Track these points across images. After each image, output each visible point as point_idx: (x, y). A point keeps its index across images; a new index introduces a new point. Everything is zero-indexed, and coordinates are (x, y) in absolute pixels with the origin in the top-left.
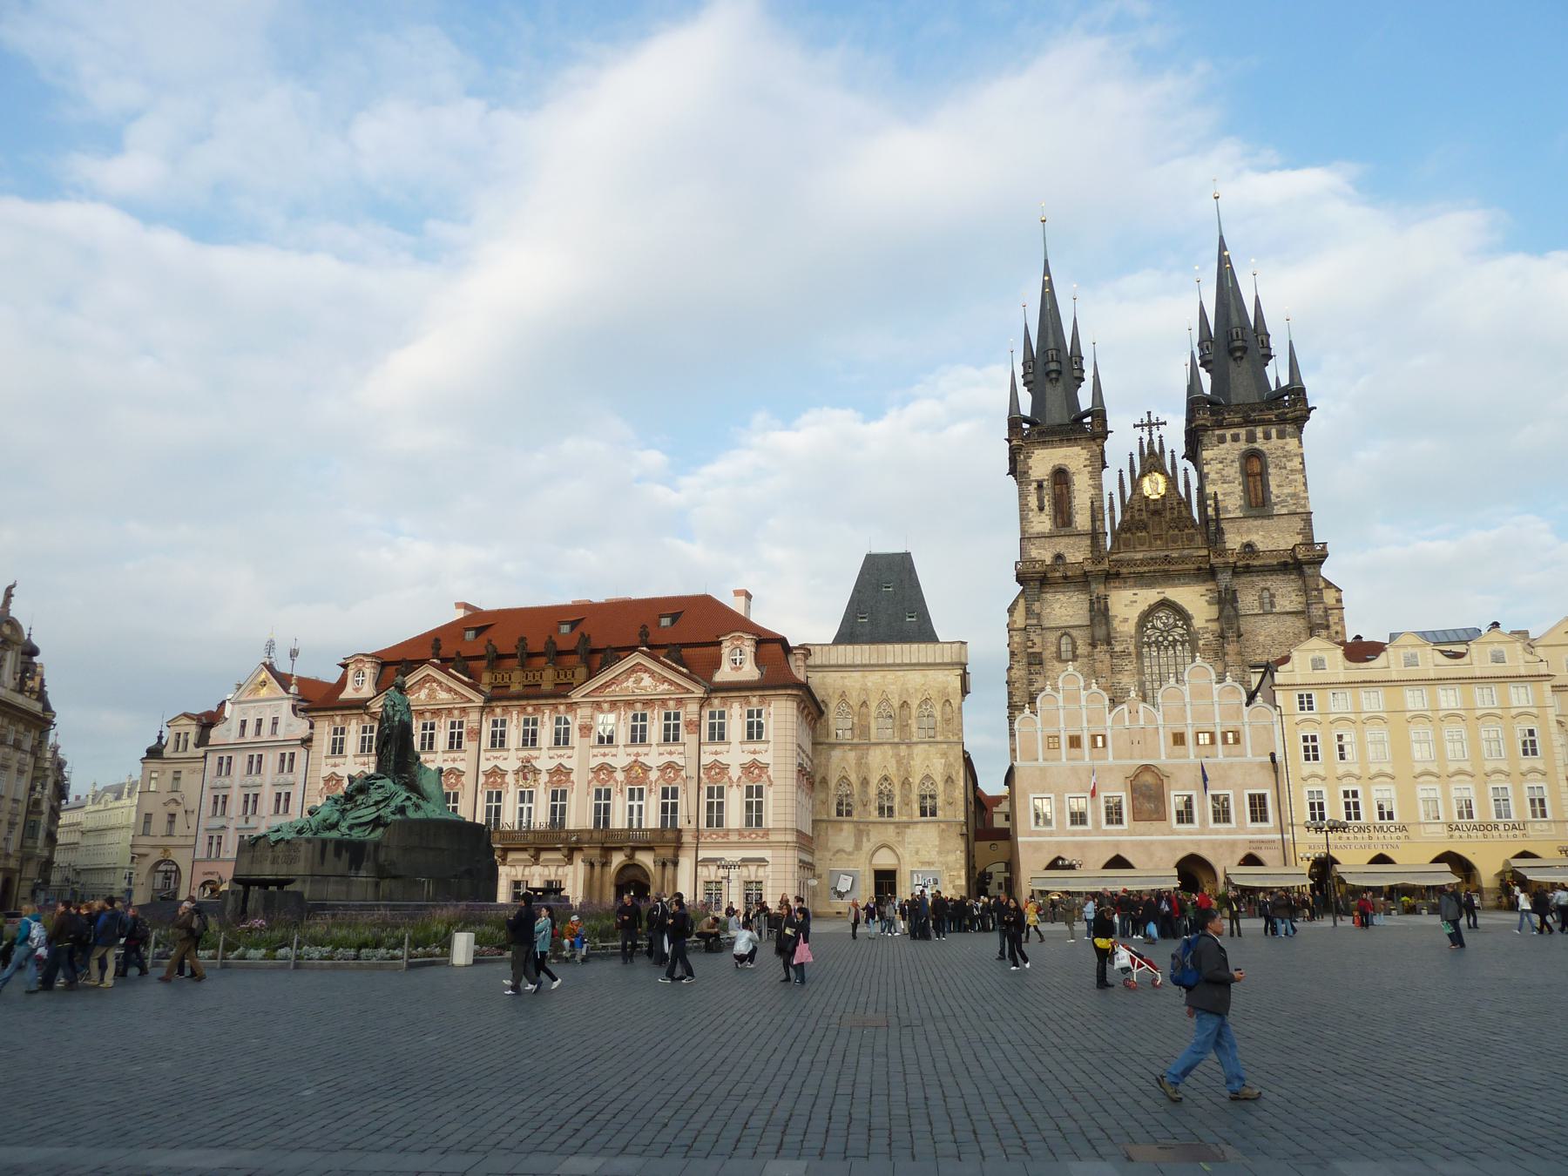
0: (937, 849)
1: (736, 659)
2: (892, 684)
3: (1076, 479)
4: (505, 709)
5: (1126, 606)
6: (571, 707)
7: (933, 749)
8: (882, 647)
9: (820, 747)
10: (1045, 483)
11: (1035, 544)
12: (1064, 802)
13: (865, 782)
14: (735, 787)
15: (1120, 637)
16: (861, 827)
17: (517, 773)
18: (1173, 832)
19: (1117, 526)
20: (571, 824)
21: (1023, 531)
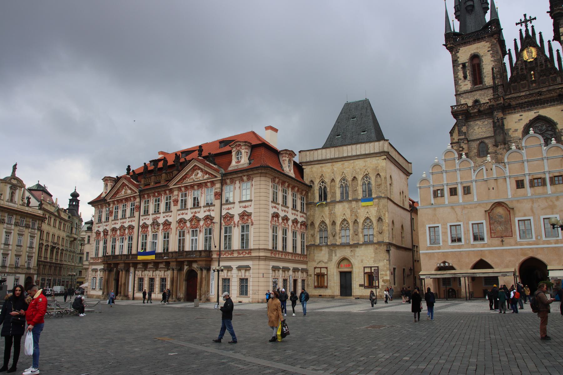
0: (373, 259)
1: (239, 157)
2: (348, 168)
3: (483, 59)
4: (149, 196)
5: (516, 122)
6: (171, 191)
8: (341, 148)
10: (467, 64)
11: (463, 97)
12: (447, 229)
13: (334, 223)
14: (236, 227)
15: (513, 140)
17: (151, 225)
18: (517, 244)
19: (509, 80)
20: (170, 250)
21: (456, 91)
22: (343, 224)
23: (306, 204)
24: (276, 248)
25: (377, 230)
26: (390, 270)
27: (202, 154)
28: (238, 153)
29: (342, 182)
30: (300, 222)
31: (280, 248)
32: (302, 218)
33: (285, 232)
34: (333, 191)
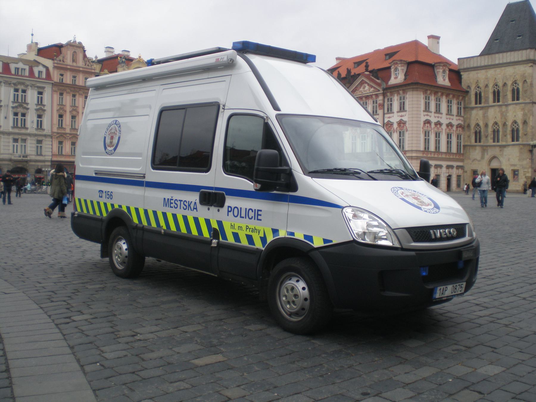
0: (518, 158)
1: (397, 73)
7: (518, 107)
8: (493, 56)
9: (467, 109)
13: (486, 125)
14: (395, 132)
16: (485, 148)
22: (495, 126)
23: (464, 108)
24: (428, 148)
25: (522, 132)
26: (532, 168)
27: (368, 70)
28: (396, 69)
29: (494, 88)
30: (457, 124)
31: (432, 148)
32: (458, 121)
33: (438, 135)
34: (487, 96)
